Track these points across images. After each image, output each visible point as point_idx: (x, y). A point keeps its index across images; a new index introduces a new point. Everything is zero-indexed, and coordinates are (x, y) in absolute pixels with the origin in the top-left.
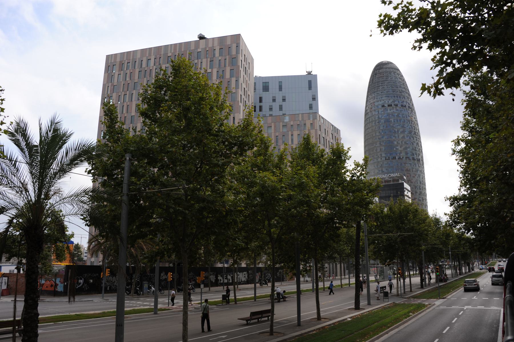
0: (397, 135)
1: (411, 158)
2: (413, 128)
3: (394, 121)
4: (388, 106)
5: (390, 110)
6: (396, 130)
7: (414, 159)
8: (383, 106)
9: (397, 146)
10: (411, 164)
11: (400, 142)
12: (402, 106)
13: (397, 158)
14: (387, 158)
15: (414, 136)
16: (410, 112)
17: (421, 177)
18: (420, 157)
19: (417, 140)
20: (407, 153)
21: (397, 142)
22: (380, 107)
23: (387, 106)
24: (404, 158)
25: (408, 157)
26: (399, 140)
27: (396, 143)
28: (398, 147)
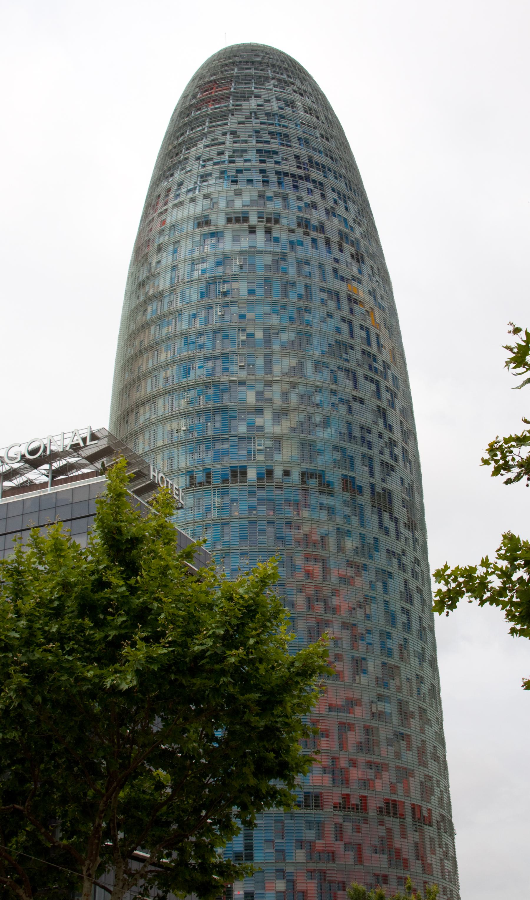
0: (260, 361)
1: (335, 476)
2: (360, 334)
3: (251, 292)
4: (229, 220)
5: (236, 239)
6: (259, 334)
7: (349, 484)
8: (203, 221)
9: (260, 411)
10: (331, 510)
11: (275, 393)
12: (304, 224)
13: (252, 474)
14: (200, 477)
15: (361, 373)
16: (345, 257)
17: (396, 585)
18: (393, 484)
19: (378, 395)
20: (308, 448)
21: (259, 395)
22: (189, 227)
23: (221, 221)
24: (295, 476)
25: (320, 476)
26: (269, 384)
27: (251, 398)
28: (265, 421)
